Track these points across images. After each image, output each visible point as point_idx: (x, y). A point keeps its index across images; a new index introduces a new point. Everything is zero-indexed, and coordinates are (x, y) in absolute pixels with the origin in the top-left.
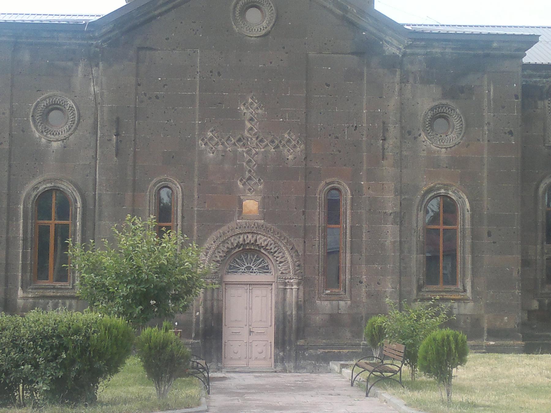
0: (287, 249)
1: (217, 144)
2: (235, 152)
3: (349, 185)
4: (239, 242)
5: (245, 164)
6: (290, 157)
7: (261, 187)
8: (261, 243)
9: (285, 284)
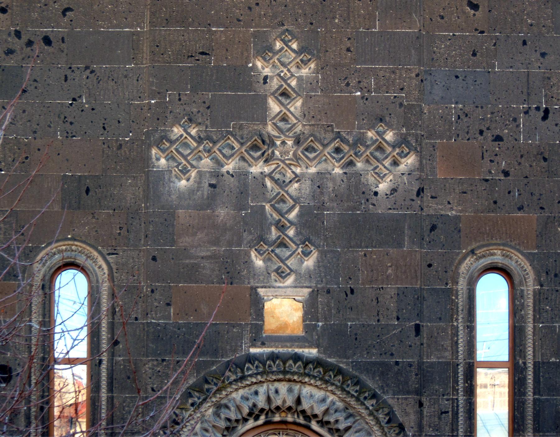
0: (378, 421)
2: (241, 175)
3: (530, 257)
4: (255, 405)
5: (268, 207)
7: (310, 263)
8: (312, 408)
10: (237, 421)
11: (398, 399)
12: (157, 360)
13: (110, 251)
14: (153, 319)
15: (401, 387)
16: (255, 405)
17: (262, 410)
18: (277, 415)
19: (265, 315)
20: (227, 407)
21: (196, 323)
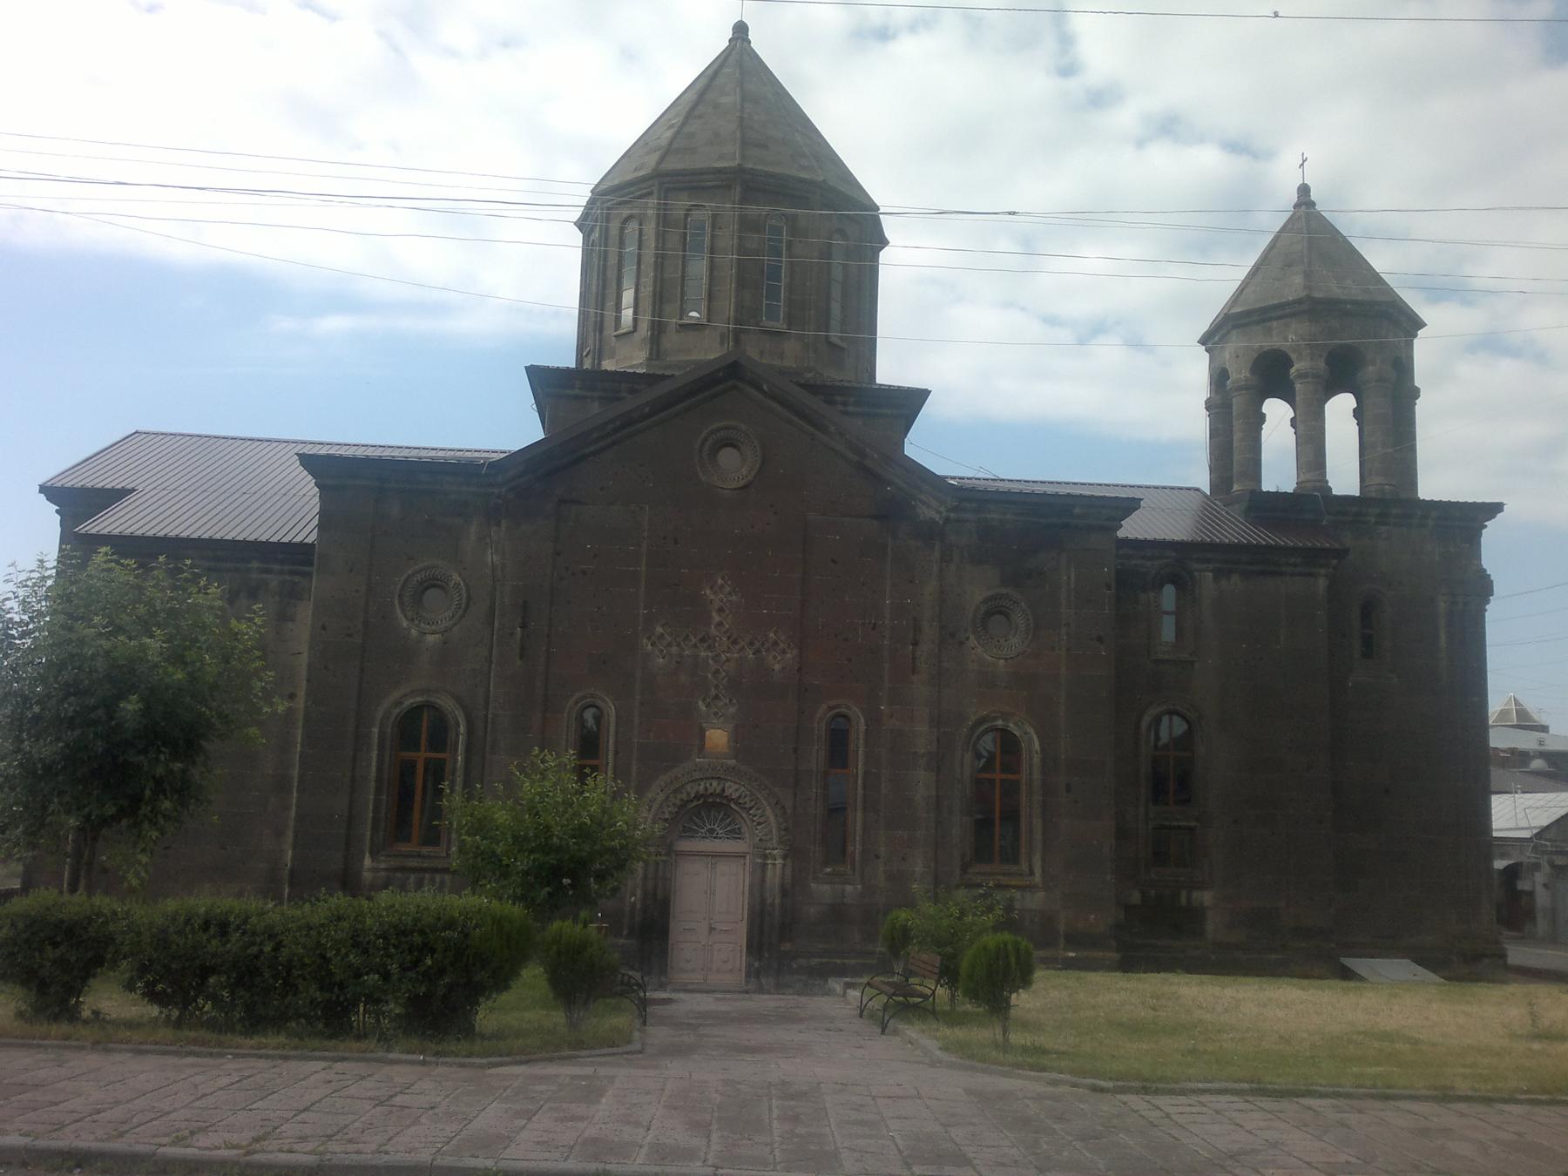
1: (670, 645)
6: (777, 667)
7: (732, 710)
9: (765, 857)
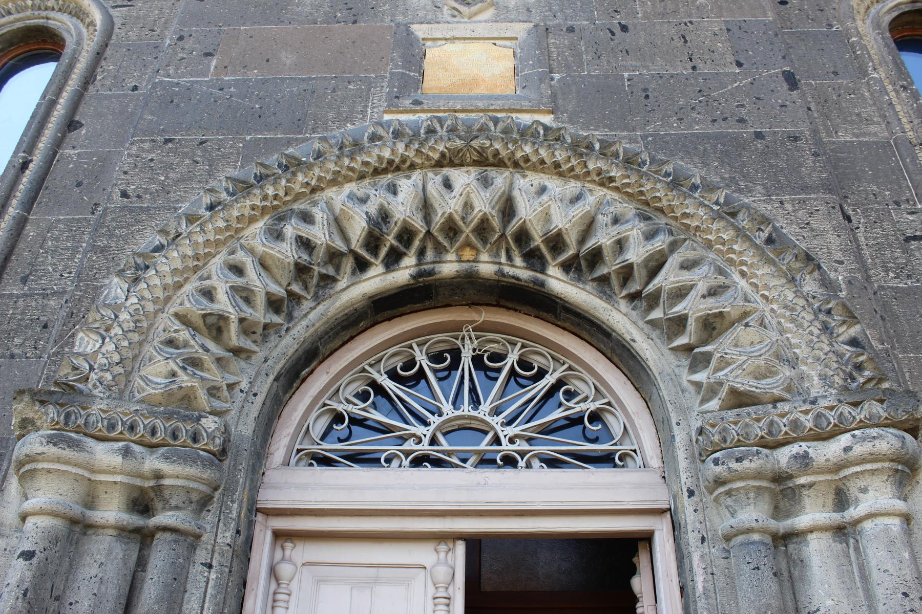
4: (384, 216)
8: (547, 218)
9: (783, 490)
10: (334, 257)
11: (781, 203)
12: (153, 141)
13: (120, 3)
14: (169, 76)
15: (782, 179)
16: (384, 216)
17: (406, 235)
18: (451, 256)
19: (427, 66)
20: (307, 218)
21: (261, 79)
